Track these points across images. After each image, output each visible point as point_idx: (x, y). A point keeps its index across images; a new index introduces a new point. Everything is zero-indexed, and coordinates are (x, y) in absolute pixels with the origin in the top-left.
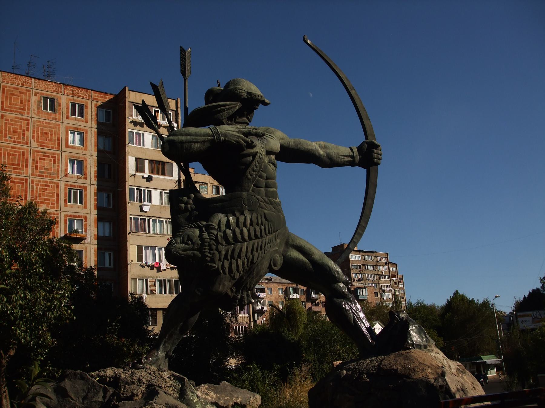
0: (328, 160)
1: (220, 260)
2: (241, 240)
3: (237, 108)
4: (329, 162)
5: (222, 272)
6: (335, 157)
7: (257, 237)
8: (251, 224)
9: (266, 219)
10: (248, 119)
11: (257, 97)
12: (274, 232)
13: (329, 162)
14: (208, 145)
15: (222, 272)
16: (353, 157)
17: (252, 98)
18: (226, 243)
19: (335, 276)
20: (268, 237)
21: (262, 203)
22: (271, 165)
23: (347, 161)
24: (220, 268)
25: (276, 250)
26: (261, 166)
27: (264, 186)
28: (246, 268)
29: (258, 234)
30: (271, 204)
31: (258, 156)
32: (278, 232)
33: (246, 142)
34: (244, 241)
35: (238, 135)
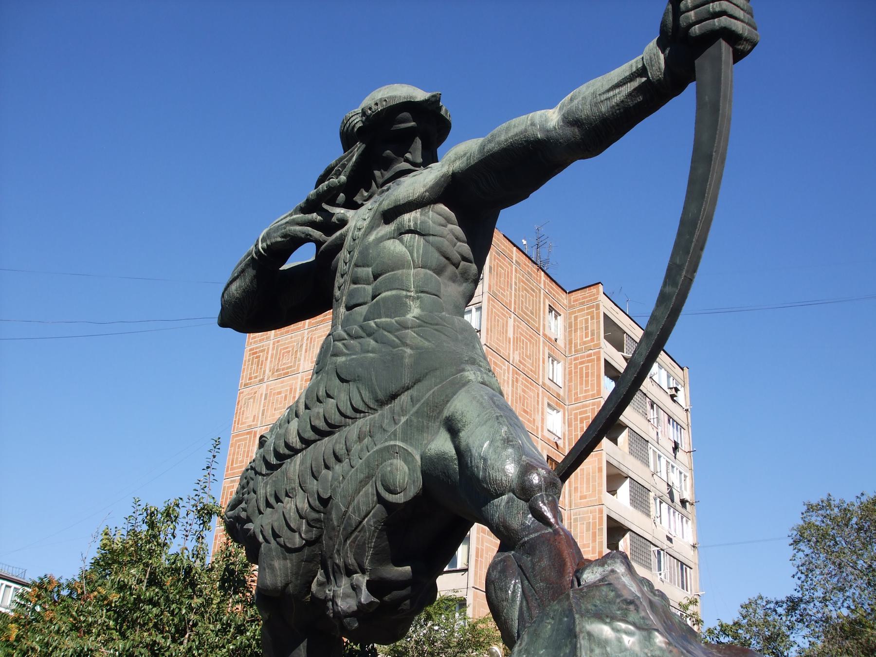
0: (569, 131)
1: (260, 513)
2: (287, 452)
3: (354, 159)
4: (595, 134)
5: (261, 539)
6: (586, 111)
7: (322, 434)
8: (307, 407)
9: (343, 380)
10: (407, 160)
11: (374, 108)
12: (382, 403)
13: (595, 134)
14: (251, 273)
15: (261, 539)
16: (643, 71)
17: (368, 117)
18: (267, 468)
19: (478, 478)
20: (360, 422)
21: (339, 344)
22: (407, 237)
23: (630, 95)
24: (258, 531)
25: (387, 448)
26: (352, 257)
27: (370, 299)
28: (315, 515)
29: (321, 425)
30: (369, 335)
31: (349, 239)
32: (404, 398)
33: (313, 224)
34: (296, 452)
35: (288, 219)
